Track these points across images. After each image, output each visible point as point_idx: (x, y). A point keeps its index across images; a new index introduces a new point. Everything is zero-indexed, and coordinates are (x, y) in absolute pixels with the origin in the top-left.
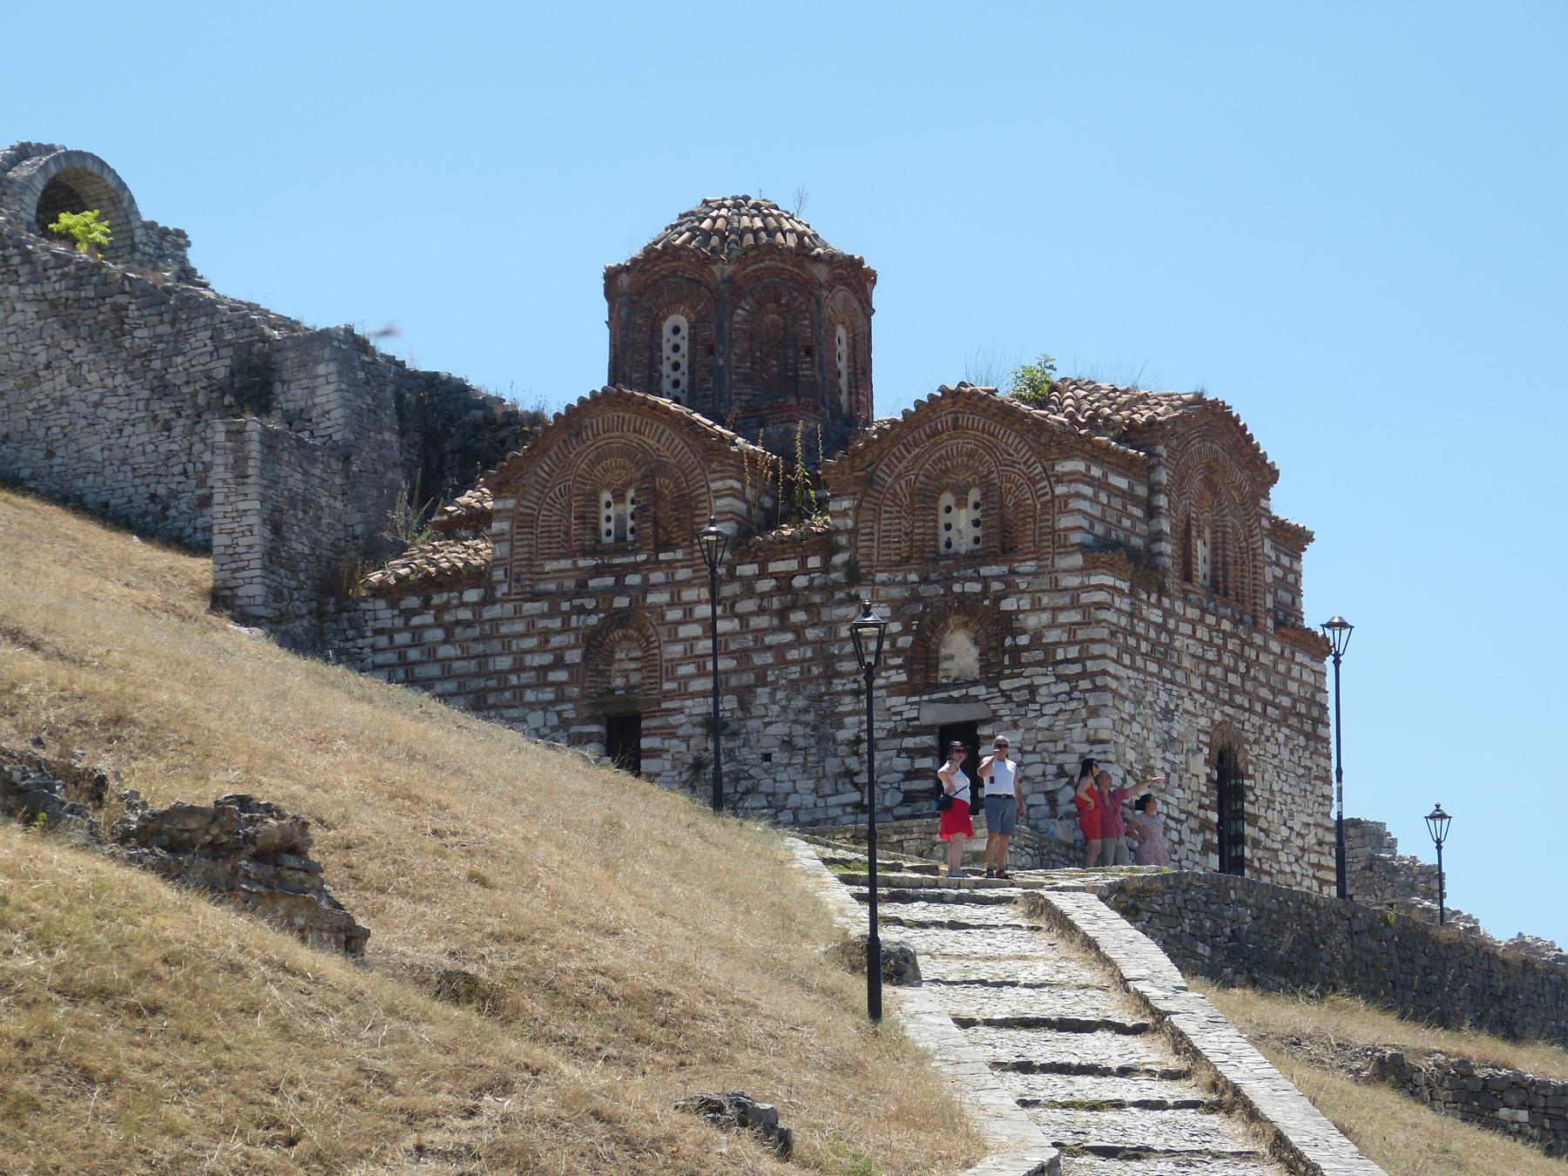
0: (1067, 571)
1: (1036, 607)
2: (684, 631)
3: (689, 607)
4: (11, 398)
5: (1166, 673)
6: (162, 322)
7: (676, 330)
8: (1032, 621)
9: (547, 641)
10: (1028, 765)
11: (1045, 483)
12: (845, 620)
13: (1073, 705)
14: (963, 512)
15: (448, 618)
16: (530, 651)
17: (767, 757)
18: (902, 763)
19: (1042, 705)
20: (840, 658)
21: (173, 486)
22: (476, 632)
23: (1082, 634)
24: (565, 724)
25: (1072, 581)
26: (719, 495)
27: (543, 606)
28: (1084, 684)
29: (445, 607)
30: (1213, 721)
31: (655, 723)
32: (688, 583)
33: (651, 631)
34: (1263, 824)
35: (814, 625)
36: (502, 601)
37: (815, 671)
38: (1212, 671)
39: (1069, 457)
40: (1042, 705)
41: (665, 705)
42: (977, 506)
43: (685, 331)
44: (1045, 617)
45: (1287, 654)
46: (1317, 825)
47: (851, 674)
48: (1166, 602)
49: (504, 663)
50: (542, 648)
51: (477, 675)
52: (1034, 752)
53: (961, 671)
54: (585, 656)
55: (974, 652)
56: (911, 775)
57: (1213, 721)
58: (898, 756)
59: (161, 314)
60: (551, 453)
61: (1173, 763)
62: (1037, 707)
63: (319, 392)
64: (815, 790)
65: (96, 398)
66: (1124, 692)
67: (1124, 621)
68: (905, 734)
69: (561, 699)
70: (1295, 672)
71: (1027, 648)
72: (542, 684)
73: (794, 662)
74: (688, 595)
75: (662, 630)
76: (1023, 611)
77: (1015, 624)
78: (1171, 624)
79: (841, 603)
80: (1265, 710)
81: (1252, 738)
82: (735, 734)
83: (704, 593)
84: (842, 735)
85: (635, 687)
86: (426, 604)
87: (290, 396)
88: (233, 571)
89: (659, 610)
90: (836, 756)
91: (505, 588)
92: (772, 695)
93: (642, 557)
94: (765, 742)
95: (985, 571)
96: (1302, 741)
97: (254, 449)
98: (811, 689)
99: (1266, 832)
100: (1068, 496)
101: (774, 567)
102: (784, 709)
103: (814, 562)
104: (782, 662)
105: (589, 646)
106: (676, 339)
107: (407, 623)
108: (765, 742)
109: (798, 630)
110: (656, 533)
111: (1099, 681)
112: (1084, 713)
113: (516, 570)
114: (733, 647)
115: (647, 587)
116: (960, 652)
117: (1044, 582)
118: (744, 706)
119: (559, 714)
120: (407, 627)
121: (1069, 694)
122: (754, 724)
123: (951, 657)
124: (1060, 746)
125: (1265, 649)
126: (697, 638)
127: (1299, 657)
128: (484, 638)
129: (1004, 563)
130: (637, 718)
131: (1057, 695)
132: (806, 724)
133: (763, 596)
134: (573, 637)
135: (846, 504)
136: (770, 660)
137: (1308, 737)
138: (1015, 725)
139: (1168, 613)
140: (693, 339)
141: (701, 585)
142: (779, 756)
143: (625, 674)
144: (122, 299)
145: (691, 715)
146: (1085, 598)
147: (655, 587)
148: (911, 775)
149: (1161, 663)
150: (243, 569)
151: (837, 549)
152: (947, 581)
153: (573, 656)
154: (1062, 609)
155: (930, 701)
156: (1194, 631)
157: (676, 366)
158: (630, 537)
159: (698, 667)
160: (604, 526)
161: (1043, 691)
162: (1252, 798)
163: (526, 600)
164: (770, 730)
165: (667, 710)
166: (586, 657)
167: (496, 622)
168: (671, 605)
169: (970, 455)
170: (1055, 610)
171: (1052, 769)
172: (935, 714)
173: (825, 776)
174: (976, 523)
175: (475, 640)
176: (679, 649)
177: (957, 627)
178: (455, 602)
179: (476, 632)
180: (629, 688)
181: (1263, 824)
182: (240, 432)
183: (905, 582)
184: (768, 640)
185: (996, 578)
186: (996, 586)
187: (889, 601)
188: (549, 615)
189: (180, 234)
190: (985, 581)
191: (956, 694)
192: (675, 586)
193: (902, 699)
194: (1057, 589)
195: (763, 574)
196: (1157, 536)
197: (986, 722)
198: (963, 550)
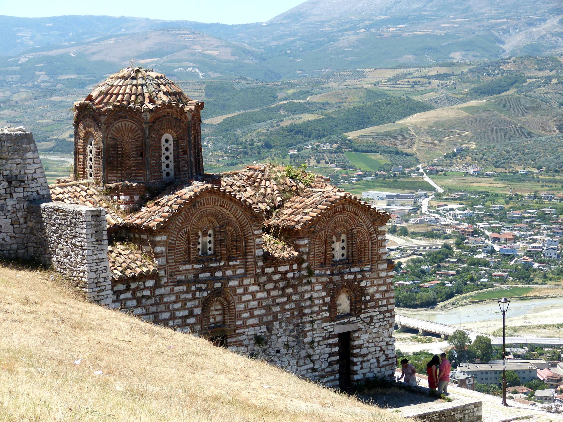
0: (383, 270)
1: (373, 285)
2: (245, 298)
3: (246, 287)
7: (167, 141)
9: (185, 304)
10: (370, 348)
11: (375, 235)
12: (307, 292)
13: (385, 323)
14: (338, 243)
15: (138, 294)
16: (178, 310)
17: (278, 351)
18: (328, 350)
19: (375, 323)
20: (305, 307)
22: (152, 301)
23: (387, 295)
25: (383, 274)
27: (184, 288)
28: (388, 315)
29: (138, 289)
31: (234, 340)
33: (231, 298)
37: (295, 313)
40: (375, 323)
41: (238, 331)
42: (343, 241)
44: (375, 288)
47: (309, 314)
50: (183, 308)
52: (372, 342)
53: (343, 310)
54: (202, 310)
55: (348, 302)
56: (331, 355)
58: (326, 347)
60: (182, 214)
62: (373, 324)
63: (28, 167)
68: (329, 338)
71: (369, 301)
73: (288, 310)
74: (246, 281)
75: (236, 298)
76: (368, 286)
77: (366, 292)
79: (305, 284)
82: (266, 343)
83: (252, 281)
84: (307, 340)
85: (218, 322)
86: (128, 289)
88: (98, 292)
89: (234, 289)
90: (304, 349)
91: (165, 280)
92: (280, 323)
93: (222, 264)
94: (278, 345)
101: (280, 269)
102: (285, 330)
103: (295, 267)
104: (284, 310)
105: (204, 306)
106: (167, 145)
107: (117, 298)
108: (278, 345)
109: (289, 296)
113: (170, 271)
114: (264, 304)
116: (344, 303)
117: (374, 275)
118: (269, 330)
121: (383, 318)
122: (273, 337)
123: (340, 305)
124: (381, 339)
126: (249, 301)
128: (156, 304)
129: (359, 266)
131: (379, 320)
132: (293, 336)
133: (277, 282)
134: (197, 302)
135: (306, 242)
136: (279, 310)
138: (366, 332)
141: (251, 277)
142: (283, 351)
145: (248, 335)
150: (103, 290)
151: (303, 261)
152: (341, 274)
153: (198, 311)
155: (337, 324)
157: (167, 158)
158: (209, 252)
159: (251, 314)
161: (375, 318)
163: (176, 286)
164: (280, 340)
165: (238, 334)
167: (162, 296)
168: (239, 286)
169: (346, 221)
170: (379, 285)
171: (378, 349)
172: (339, 329)
173: (300, 358)
174: (343, 248)
175: (152, 305)
176: (241, 306)
178: (142, 287)
179: (152, 301)
182: (98, 216)
184: (278, 301)
186: (359, 276)
188: (186, 292)
190: (355, 273)
191: (346, 320)
193: (328, 324)
195: (276, 272)
197: (355, 331)
198: (338, 259)
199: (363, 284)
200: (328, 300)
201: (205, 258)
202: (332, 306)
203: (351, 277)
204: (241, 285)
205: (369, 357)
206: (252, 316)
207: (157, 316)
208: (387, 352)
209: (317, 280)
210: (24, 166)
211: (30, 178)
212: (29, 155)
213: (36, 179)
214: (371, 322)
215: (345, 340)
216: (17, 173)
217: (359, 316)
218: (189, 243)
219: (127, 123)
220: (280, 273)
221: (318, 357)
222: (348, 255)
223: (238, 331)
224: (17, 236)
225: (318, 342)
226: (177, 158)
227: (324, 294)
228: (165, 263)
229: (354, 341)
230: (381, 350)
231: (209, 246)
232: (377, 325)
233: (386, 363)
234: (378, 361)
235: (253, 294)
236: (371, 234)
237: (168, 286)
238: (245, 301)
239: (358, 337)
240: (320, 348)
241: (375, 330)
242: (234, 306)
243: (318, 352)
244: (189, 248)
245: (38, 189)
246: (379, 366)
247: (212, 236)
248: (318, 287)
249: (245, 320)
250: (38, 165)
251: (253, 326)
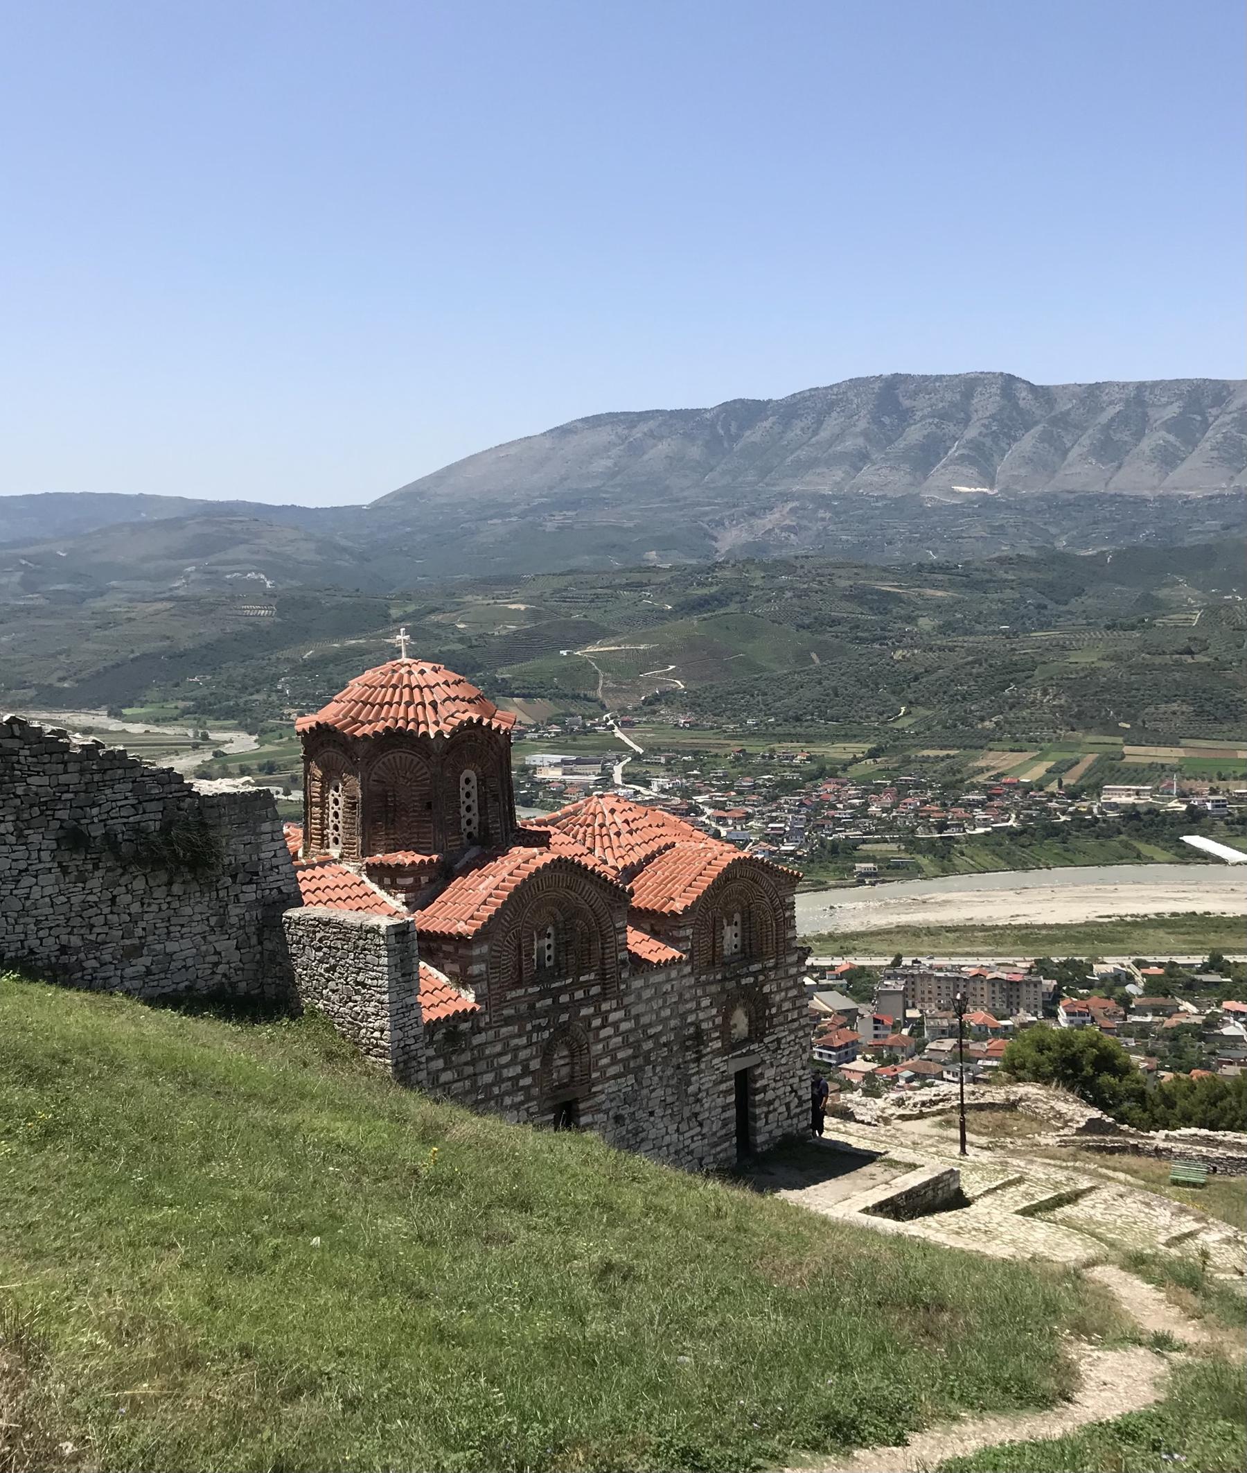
0: (792, 965)
1: (780, 990)
6: (66, 772)
7: (468, 781)
12: (691, 1012)
16: (507, 1066)
17: (652, 1114)
18: (720, 1101)
21: (93, 937)
25: (793, 971)
28: (801, 1033)
36: (485, 1030)
41: (594, 1090)
43: (474, 782)
55: (746, 1020)
56: (725, 1108)
59: (65, 763)
63: (264, 847)
64: (678, 1130)
68: (721, 1082)
69: (528, 1099)
71: (775, 1015)
72: (516, 1089)
89: (588, 1019)
98: (674, 1061)
102: (661, 1078)
105: (545, 1054)
106: (468, 788)
115: (577, 1004)
116: (741, 1022)
117: (781, 973)
119: (527, 1110)
122: (645, 1092)
123: (735, 1026)
126: (609, 1037)
128: (473, 1062)
153: (535, 1065)
157: (469, 809)
158: (548, 964)
163: (501, 1026)
168: (594, 1015)
171: (789, 1089)
175: (466, 1064)
176: (600, 1046)
188: (520, 1036)
195: (647, 986)
197: (758, 1066)
199: (766, 989)
200: (719, 1020)
201: (542, 975)
202: (725, 1028)
203: (751, 980)
204: (598, 1013)
205: (777, 1104)
206: (614, 1061)
207: (476, 1081)
208: (800, 1093)
209: (704, 991)
210: (258, 847)
211: (268, 866)
212: (266, 827)
213: (277, 867)
215: (744, 1081)
216: (245, 858)
217: (762, 1041)
218: (520, 954)
219: (404, 755)
221: (707, 1115)
222: (743, 945)
223: (594, 1090)
224: (246, 967)
225: (707, 1090)
226: (482, 808)
228: (486, 991)
229: (756, 1082)
231: (548, 953)
233: (798, 1110)
234: (788, 1109)
235: (616, 1025)
236: (775, 910)
237: (491, 1028)
238: (605, 1039)
240: (710, 1099)
242: (588, 1048)
243: (706, 1106)
244: (520, 961)
245: (280, 883)
246: (789, 1117)
247: (552, 937)
248: (705, 1002)
249: (603, 1070)
250: (280, 844)
251: (615, 1077)
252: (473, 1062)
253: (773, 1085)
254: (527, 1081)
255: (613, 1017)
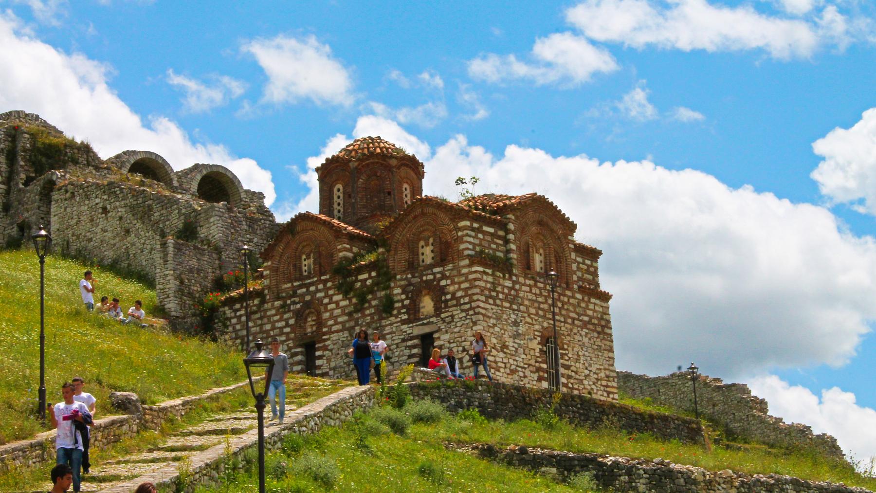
0: (464, 267)
1: (453, 283)
2: (330, 307)
3: (331, 297)
4: (118, 245)
5: (515, 307)
7: (339, 190)
8: (451, 289)
13: (468, 321)
18: (407, 352)
23: (470, 292)
24: (290, 349)
25: (465, 271)
26: (340, 251)
28: (471, 312)
30: (543, 327)
32: (330, 288)
34: (573, 368)
35: (374, 299)
37: (376, 318)
38: (542, 306)
39: (463, 220)
43: (341, 190)
44: (456, 286)
45: (586, 299)
46: (605, 369)
48: (514, 278)
49: (268, 327)
51: (260, 333)
55: (432, 304)
57: (543, 327)
61: (519, 344)
65: (143, 241)
66: (490, 315)
67: (489, 286)
70: (591, 306)
73: (368, 315)
74: (331, 292)
78: (517, 287)
80: (573, 322)
81: (566, 333)
87: (203, 232)
89: (320, 300)
93: (315, 279)
95: (435, 270)
96: (596, 335)
97: (171, 249)
98: (374, 325)
99: (576, 373)
100: (463, 236)
101: (361, 277)
106: (339, 194)
110: (320, 269)
111: (477, 310)
112: (471, 324)
114: (347, 311)
116: (427, 304)
117: (455, 273)
120: (236, 317)
123: (424, 307)
125: (573, 297)
126: (334, 309)
127: (593, 300)
128: (261, 318)
130: (314, 343)
137: (599, 333)
138: (447, 332)
139: (514, 283)
140: (344, 193)
143: (312, 326)
144: (150, 202)
146: (471, 277)
147: (320, 291)
148: (410, 356)
149: (511, 303)
152: (421, 277)
153: (292, 322)
154: (462, 282)
156: (531, 290)
160: (305, 268)
161: (456, 317)
162: (567, 358)
166: (296, 321)
168: (325, 297)
170: (460, 283)
171: (461, 349)
172: (418, 330)
175: (258, 319)
176: (327, 315)
177: (426, 295)
180: (312, 333)
181: (573, 368)
183: (406, 279)
185: (438, 273)
186: (438, 276)
187: (400, 286)
189: (261, 193)
190: (434, 274)
191: (425, 322)
192: (326, 289)
194: (461, 275)
196: (509, 251)
199: (443, 283)
206: (336, 323)
214: (453, 321)
220: (361, 281)
221: (396, 359)
225: (397, 344)
227: (403, 297)
230: (464, 350)
232: (459, 324)
235: (337, 303)
239: (439, 338)
241: (456, 330)
243: (397, 354)
252: (261, 318)
253: (448, 345)
254: (287, 330)
255: (336, 298)
